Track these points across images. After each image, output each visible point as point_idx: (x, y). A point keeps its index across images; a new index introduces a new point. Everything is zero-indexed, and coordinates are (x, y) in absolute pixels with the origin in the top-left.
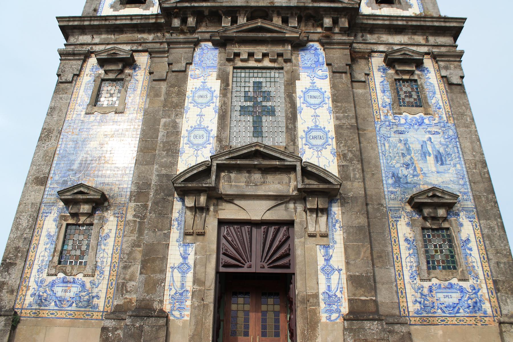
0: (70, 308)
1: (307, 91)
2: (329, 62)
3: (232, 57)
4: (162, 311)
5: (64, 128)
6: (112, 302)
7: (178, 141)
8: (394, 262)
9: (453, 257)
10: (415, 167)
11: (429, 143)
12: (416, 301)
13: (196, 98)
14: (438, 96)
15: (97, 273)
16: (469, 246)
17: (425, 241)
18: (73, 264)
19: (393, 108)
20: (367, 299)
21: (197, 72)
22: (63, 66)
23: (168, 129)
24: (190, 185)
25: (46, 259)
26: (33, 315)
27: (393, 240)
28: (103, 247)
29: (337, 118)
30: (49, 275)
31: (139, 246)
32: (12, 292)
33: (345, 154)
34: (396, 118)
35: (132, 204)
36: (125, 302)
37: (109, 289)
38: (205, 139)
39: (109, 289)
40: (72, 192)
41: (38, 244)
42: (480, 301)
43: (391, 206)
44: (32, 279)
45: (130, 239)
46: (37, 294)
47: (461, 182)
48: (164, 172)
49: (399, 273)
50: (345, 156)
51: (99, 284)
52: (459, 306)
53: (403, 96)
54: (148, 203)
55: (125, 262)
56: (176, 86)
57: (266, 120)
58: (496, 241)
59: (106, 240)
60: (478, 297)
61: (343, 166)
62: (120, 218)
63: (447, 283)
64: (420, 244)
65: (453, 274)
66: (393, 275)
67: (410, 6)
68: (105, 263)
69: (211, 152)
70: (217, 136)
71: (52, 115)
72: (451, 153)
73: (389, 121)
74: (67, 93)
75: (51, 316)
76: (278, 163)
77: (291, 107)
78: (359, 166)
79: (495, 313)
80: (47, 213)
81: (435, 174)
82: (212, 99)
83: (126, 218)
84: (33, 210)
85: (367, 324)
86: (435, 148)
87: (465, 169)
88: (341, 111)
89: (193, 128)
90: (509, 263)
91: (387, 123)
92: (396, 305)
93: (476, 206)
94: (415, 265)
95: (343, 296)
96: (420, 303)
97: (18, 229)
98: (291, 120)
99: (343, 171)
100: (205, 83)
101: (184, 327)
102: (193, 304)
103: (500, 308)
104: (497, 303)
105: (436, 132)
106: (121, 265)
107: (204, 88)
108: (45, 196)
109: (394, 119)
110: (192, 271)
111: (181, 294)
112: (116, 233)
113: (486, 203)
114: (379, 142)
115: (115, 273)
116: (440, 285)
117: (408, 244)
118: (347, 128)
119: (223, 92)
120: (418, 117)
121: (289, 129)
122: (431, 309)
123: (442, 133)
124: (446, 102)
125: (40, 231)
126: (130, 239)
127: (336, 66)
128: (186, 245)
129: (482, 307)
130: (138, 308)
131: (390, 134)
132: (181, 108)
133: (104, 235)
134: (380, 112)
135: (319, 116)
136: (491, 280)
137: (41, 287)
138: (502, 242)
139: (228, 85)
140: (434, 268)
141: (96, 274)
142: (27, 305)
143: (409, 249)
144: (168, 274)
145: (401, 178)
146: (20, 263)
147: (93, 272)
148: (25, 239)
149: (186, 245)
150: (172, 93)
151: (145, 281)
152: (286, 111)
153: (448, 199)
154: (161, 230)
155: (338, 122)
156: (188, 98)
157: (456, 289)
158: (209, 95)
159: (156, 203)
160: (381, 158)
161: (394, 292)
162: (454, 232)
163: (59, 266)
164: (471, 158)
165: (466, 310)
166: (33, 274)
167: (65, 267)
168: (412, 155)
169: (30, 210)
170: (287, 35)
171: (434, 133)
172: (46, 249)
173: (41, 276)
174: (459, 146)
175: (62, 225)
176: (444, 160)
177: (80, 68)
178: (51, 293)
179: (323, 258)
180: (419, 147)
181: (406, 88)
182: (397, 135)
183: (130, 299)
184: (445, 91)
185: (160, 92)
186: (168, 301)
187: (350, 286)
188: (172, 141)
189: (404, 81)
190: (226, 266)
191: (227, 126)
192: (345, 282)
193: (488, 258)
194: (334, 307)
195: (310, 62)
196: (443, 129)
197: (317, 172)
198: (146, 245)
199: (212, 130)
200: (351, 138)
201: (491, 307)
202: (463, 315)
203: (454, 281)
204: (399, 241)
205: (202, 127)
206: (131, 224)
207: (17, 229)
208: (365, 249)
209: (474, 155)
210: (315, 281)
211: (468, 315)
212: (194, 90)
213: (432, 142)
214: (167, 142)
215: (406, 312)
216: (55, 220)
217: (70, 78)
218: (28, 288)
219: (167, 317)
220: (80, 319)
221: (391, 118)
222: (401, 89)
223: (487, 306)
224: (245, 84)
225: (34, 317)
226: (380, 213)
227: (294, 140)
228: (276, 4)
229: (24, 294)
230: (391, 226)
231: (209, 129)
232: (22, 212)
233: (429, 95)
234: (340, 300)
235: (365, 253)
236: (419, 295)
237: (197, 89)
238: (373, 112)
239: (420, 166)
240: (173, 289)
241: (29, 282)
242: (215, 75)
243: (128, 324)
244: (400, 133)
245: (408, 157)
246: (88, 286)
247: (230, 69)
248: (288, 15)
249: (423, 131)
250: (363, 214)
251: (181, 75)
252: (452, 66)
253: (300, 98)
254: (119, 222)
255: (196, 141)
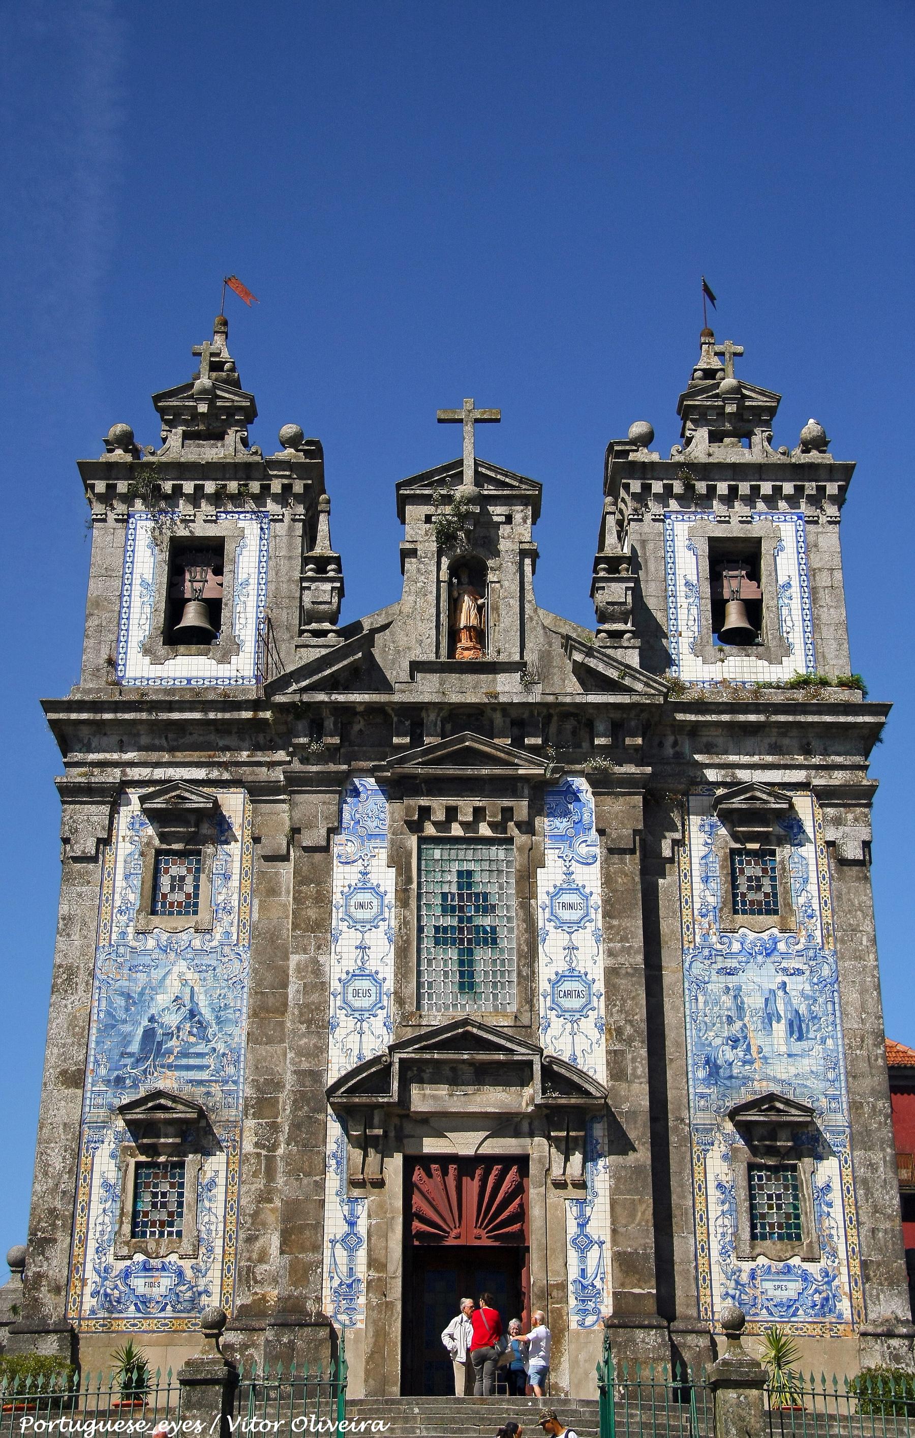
0: (162, 1315)
1: (558, 893)
2: (600, 827)
3: (416, 817)
4: (320, 1314)
5: (99, 964)
6: (233, 1301)
7: (325, 1002)
8: (695, 1226)
9: (797, 1217)
10: (749, 1045)
11: (780, 993)
12: (727, 1294)
13: (352, 909)
14: (812, 888)
15: (203, 1250)
16: (827, 1198)
17: (751, 1188)
18: (157, 1236)
19: (721, 917)
20: (643, 1292)
21: (350, 848)
22: (71, 818)
23: (304, 977)
24: (357, 1100)
25: (109, 1229)
26: (101, 1329)
27: (696, 1186)
28: (207, 1204)
29: (611, 953)
30: (118, 1258)
31: (270, 1201)
32: (57, 1290)
33: (619, 1027)
34: (725, 940)
35: (250, 1123)
36: (254, 1300)
37: (225, 1279)
38: (373, 998)
39: (225, 1279)
40: (143, 1108)
41: (90, 1202)
42: (834, 1296)
43: (699, 1121)
44: (89, 1266)
45: (253, 1187)
46: (102, 1292)
47: (831, 1075)
48: (305, 1066)
49: (702, 1246)
50: (619, 1031)
51: (207, 1270)
52: (797, 1304)
53: (743, 889)
54: (279, 1120)
55: (249, 1230)
56: (312, 882)
57: (482, 955)
58: (877, 1190)
59: (210, 1191)
60: (831, 1290)
61: (615, 1051)
62: (231, 1149)
63: (782, 1264)
64: (743, 1194)
65: (793, 1248)
66: (693, 1248)
67: (787, 650)
68: (214, 1233)
69: (385, 1023)
70: (395, 993)
71: (68, 935)
72: (819, 1016)
73: (710, 947)
74: (89, 882)
75: (132, 1329)
76: (502, 1057)
77: (526, 930)
78: (644, 1052)
79: (856, 1317)
80: (95, 1142)
81: (785, 1059)
82: (382, 913)
83: (241, 1149)
84: (69, 1137)
85: (640, 1334)
86: (791, 1005)
87: (840, 1049)
88: (618, 938)
89: (350, 975)
90: (893, 1230)
91: (706, 952)
92: (693, 1301)
93: (850, 1123)
94: (730, 1231)
95: (605, 1287)
96: (733, 1297)
97: (47, 1174)
98: (526, 958)
99: (615, 1062)
100: (367, 874)
101: (357, 1340)
102: (369, 1302)
103: (866, 1309)
104: (862, 1301)
105: (798, 969)
106: (242, 1235)
107: (365, 885)
108: (87, 1109)
109: (721, 943)
110: (365, 1246)
111: (350, 1286)
112: (227, 1178)
113: (870, 1117)
114: (687, 992)
115: (232, 1251)
116: (770, 1267)
117: (723, 1193)
118: (627, 973)
119: (402, 895)
120: (766, 938)
121: (523, 976)
122: (750, 1309)
123: (808, 973)
124: (826, 902)
125: (88, 1177)
126: (253, 1187)
127: (614, 835)
128: (353, 1201)
129: (835, 1306)
130: (284, 1311)
131: (710, 977)
132: (326, 932)
133: (206, 1181)
134: (694, 928)
135: (577, 949)
136: (857, 1261)
137: (106, 1279)
138: (888, 1193)
139: (409, 880)
140: (764, 1237)
141: (200, 1252)
142: (88, 1312)
143: (723, 1203)
144: (327, 1253)
145: (720, 1067)
146: (63, 1241)
147: (194, 1251)
148: (64, 1193)
149: (353, 1201)
150: (306, 898)
151: (290, 1265)
152: (518, 939)
153: (796, 1116)
154: (308, 1175)
155: (611, 962)
156: (338, 909)
157: (796, 1274)
158: (375, 903)
159: (296, 1126)
160: (688, 1027)
161: (692, 1278)
162: (805, 1173)
163: (134, 1240)
164: (856, 1026)
165: (808, 1311)
166: (88, 1258)
167: (143, 1242)
168: (746, 1019)
169: (63, 1137)
170: (520, 772)
171: (792, 971)
172: (104, 1210)
173: (103, 1259)
174: (836, 1000)
175: (127, 1165)
176: (804, 1030)
177: (107, 822)
178: (127, 1289)
179: (575, 1223)
180: (759, 1002)
181: (752, 870)
182: (722, 978)
183: (263, 1295)
184: (827, 876)
185: (278, 883)
186: (329, 1298)
187: (617, 1270)
188: (313, 1003)
189: (749, 853)
190: (421, 1235)
191: (413, 973)
192: (610, 1263)
193: (857, 1220)
194: (591, 1305)
195: (565, 824)
196: (811, 963)
197: (568, 1074)
198: (287, 1202)
199: (385, 979)
200: (633, 994)
201: (852, 1306)
202: (802, 1320)
203: (796, 1261)
204: (706, 1188)
205: (367, 972)
206: (253, 1161)
207: (46, 1174)
208: (644, 1206)
209: (862, 1020)
210: (561, 1262)
211: (810, 1320)
212: (346, 890)
213: (786, 993)
214: (307, 1005)
215: (709, 1313)
216: (113, 1156)
217: (90, 847)
218: (84, 1281)
219: (331, 1325)
220: (181, 1331)
221: (714, 939)
222: (742, 871)
223: (844, 1306)
224: (442, 876)
225: (103, 1332)
226: (677, 1136)
227: (532, 1000)
228: (503, 699)
229: (79, 1292)
230: (695, 1160)
231: (380, 976)
232: (48, 1141)
233: (796, 885)
234: (599, 1293)
235: (643, 1213)
236: (733, 1284)
237: (352, 888)
238: (682, 928)
239: (759, 1042)
240: (336, 1277)
241: (84, 1271)
242: (383, 855)
243: (270, 1338)
244: (729, 974)
245: (738, 1024)
246: (189, 1273)
247: (413, 841)
248: (525, 716)
249: (770, 968)
250: (645, 1143)
251: (318, 856)
252: (850, 816)
253: (544, 910)
254: (231, 1157)
255: (357, 1003)
